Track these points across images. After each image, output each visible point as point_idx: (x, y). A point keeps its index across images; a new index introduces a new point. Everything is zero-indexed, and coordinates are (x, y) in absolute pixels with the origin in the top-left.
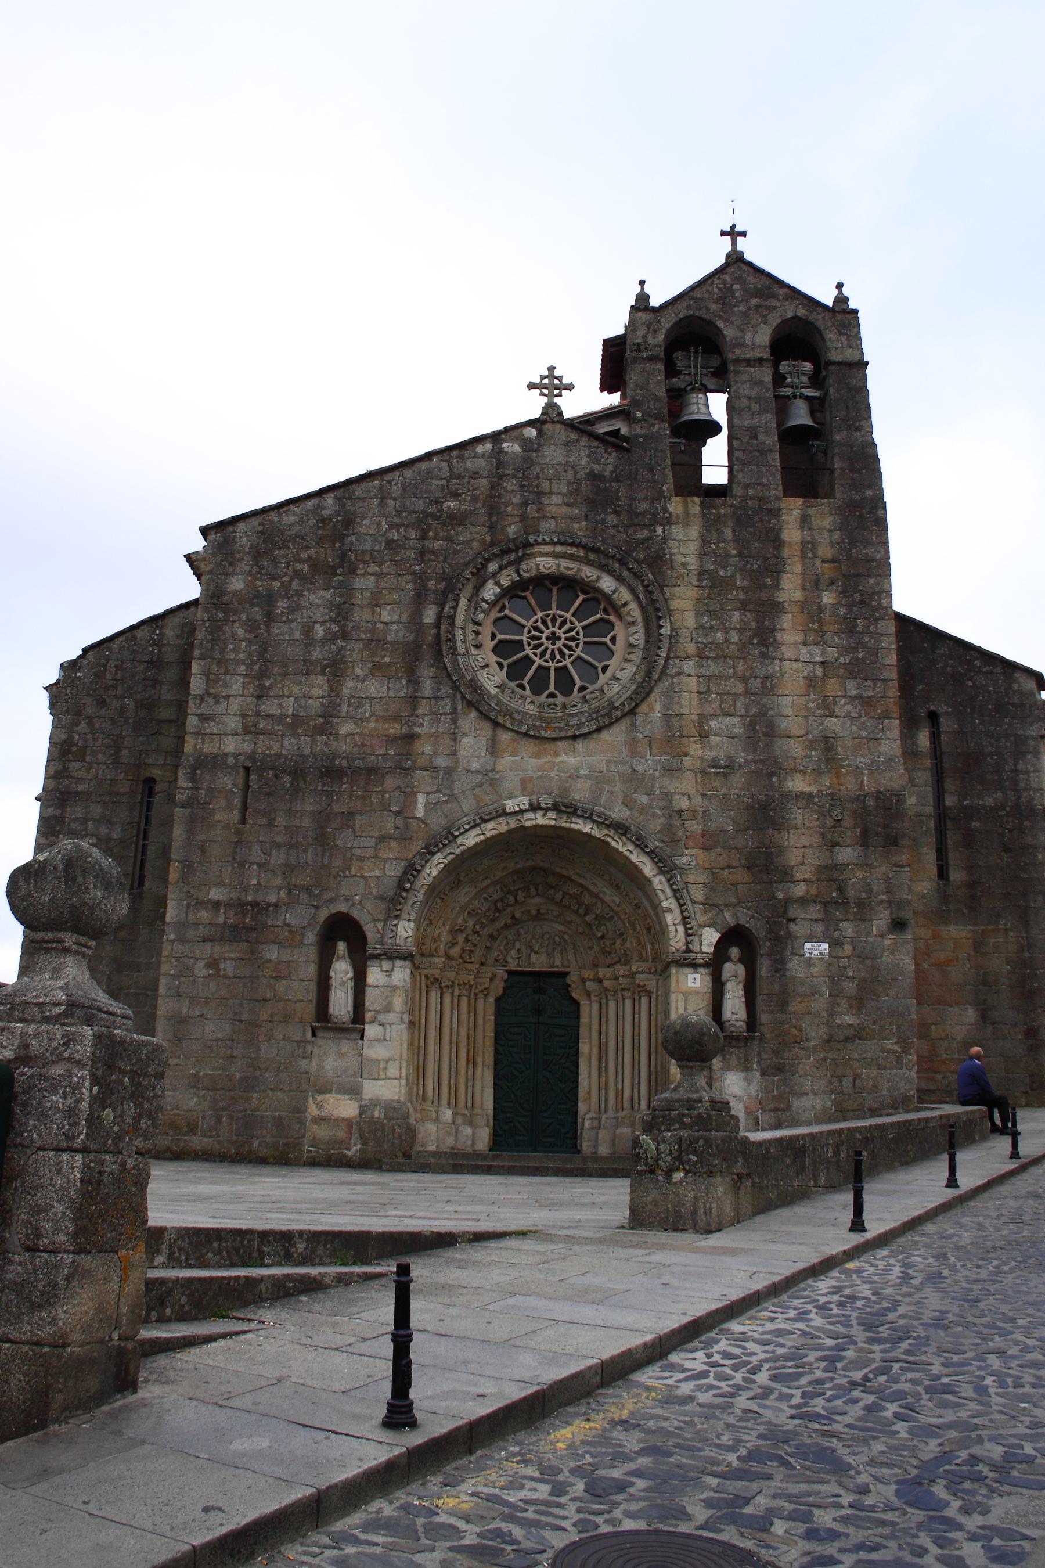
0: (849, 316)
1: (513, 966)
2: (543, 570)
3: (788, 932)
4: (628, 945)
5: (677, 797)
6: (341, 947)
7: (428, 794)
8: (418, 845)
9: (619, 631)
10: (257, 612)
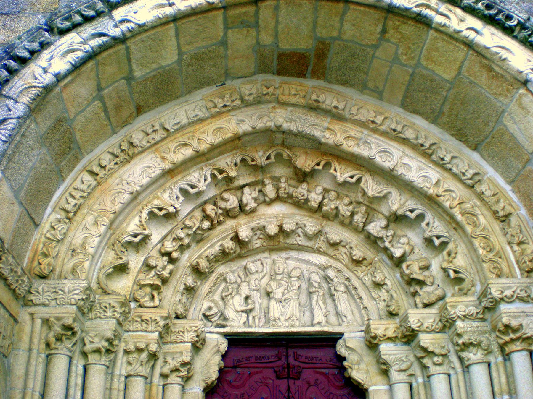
1: (237, 325)
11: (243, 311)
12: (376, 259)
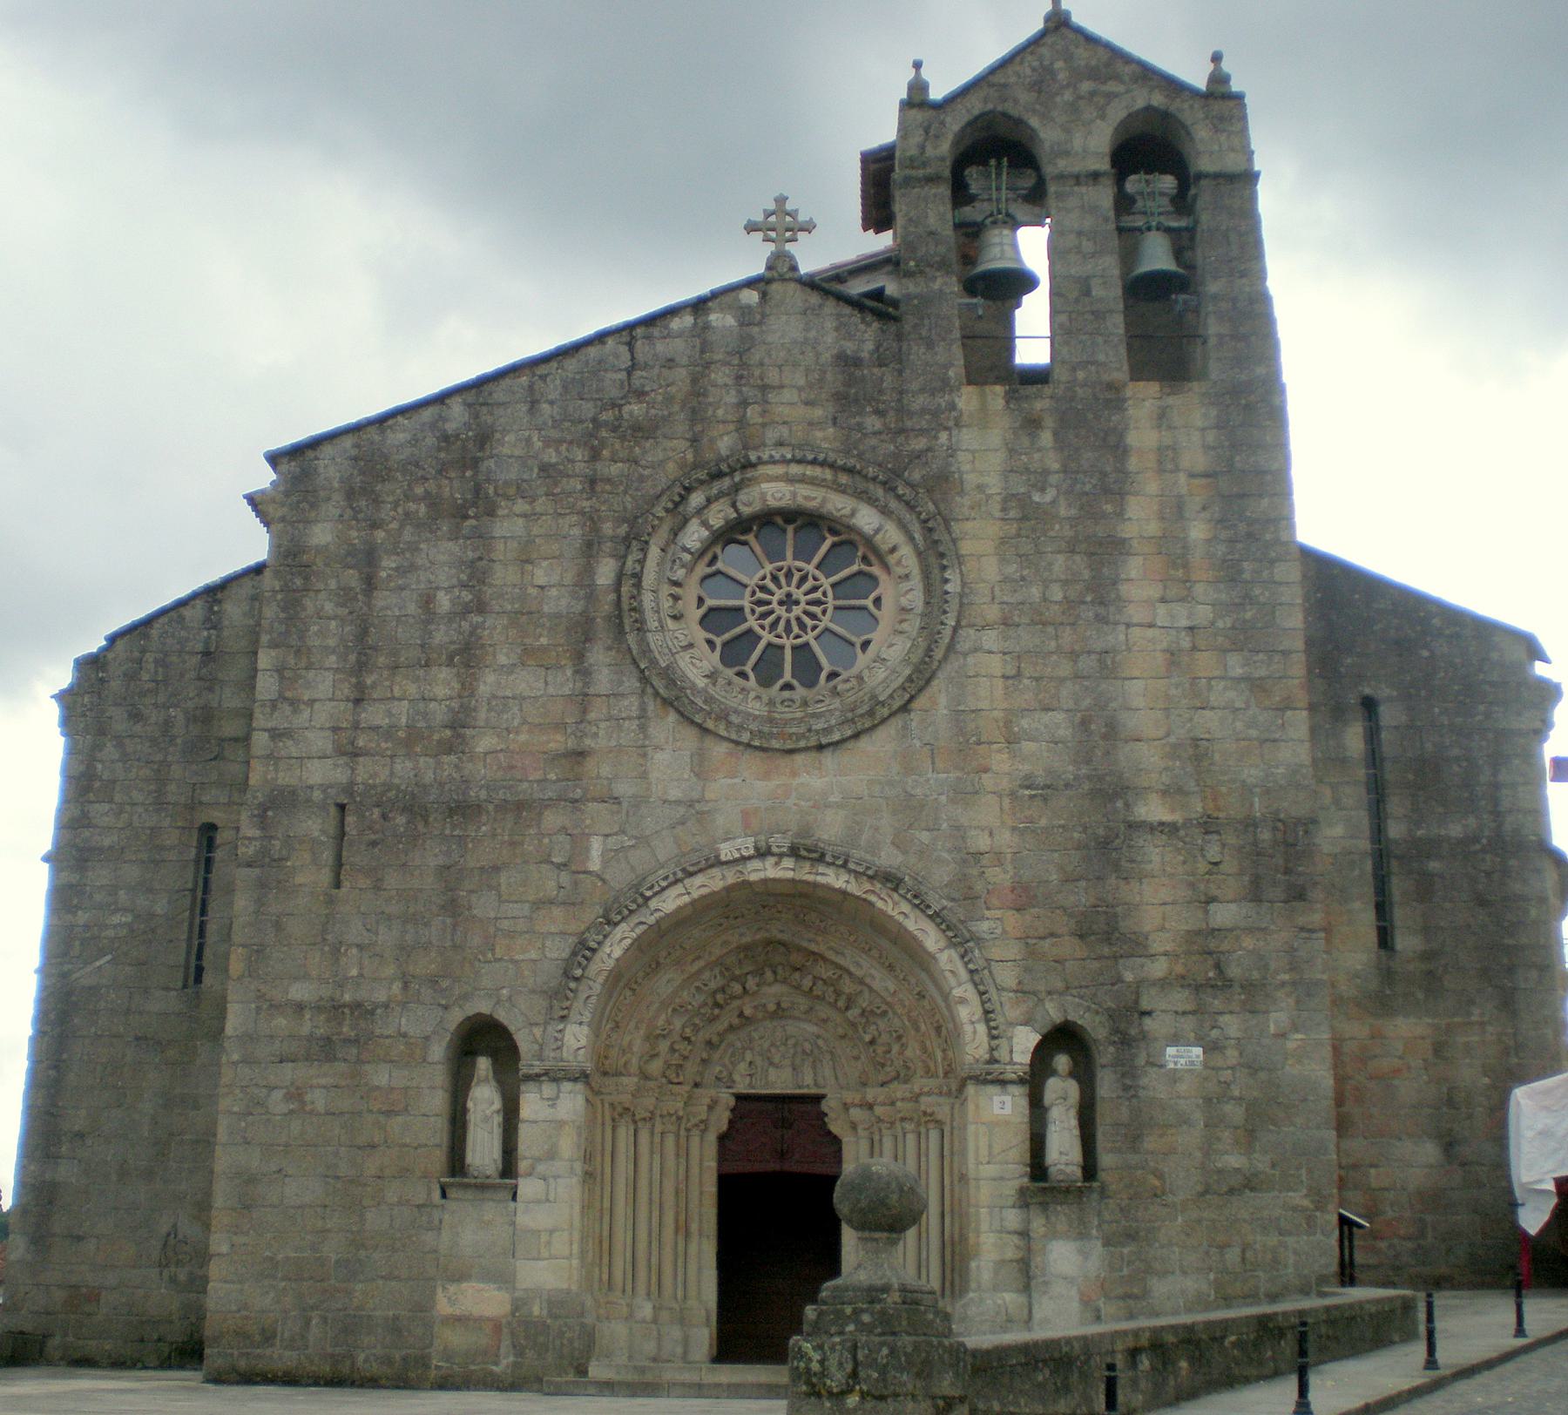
0: (1231, 104)
1: (742, 1088)
2: (773, 503)
3: (1142, 1031)
4: (909, 1053)
5: (973, 833)
6: (483, 1064)
7: (607, 836)
8: (592, 913)
9: (886, 588)
10: (352, 578)
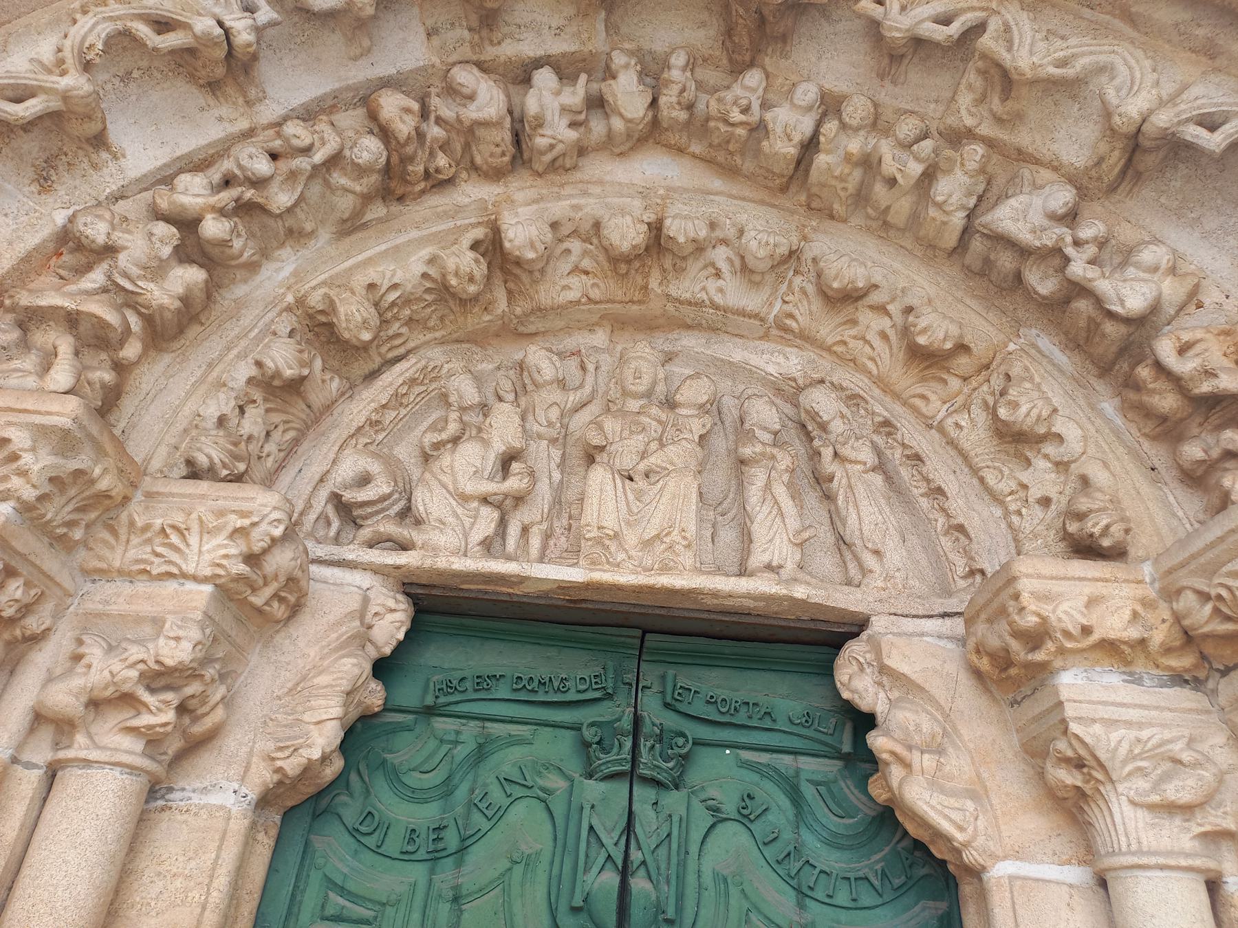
1: (452, 546)
11: (485, 500)
12: (1012, 347)
